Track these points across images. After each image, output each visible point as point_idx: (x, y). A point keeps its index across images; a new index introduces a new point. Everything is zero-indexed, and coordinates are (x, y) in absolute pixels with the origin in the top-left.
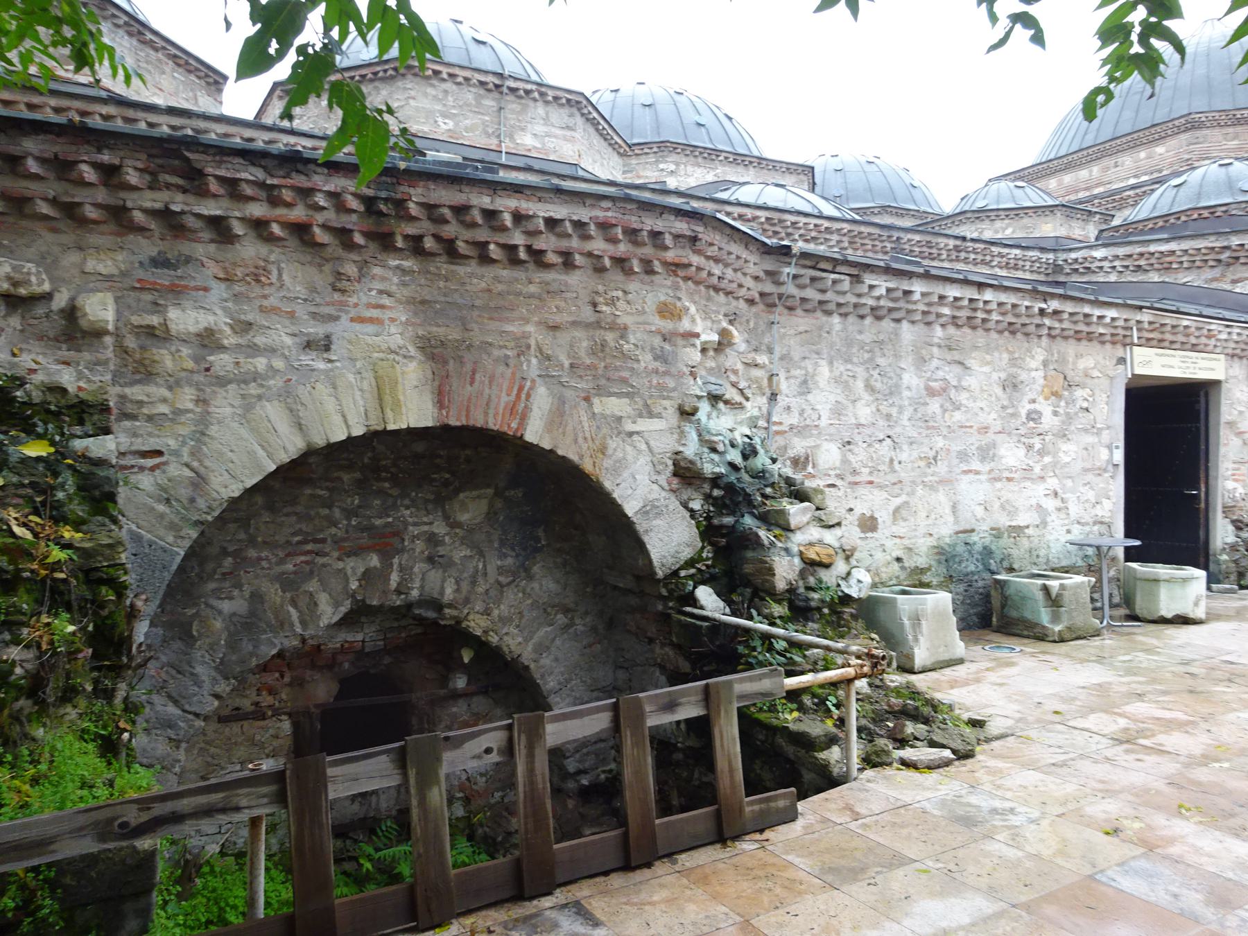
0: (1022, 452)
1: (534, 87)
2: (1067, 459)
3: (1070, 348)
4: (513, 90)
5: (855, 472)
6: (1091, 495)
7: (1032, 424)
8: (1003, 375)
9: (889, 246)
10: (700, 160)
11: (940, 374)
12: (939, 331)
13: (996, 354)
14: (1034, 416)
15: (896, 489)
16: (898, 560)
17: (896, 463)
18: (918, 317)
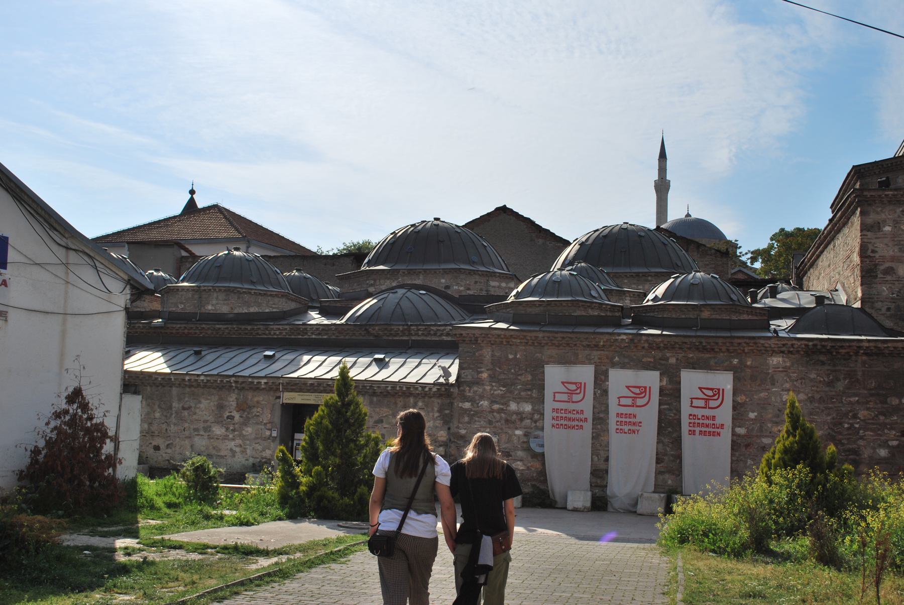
0: (223, 430)
1: (211, 288)
2: (247, 434)
3: (250, 395)
4: (205, 290)
5: (152, 432)
6: (260, 448)
7: (229, 420)
8: (216, 403)
9: (363, 333)
10: (389, 276)
11: (188, 403)
12: (188, 389)
13: (213, 396)
14: (231, 418)
15: (169, 438)
16: (168, 460)
17: (168, 430)
18: (177, 385)
